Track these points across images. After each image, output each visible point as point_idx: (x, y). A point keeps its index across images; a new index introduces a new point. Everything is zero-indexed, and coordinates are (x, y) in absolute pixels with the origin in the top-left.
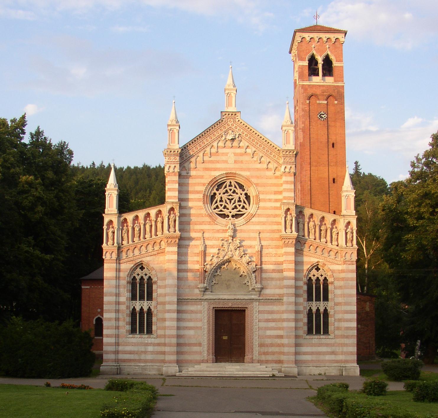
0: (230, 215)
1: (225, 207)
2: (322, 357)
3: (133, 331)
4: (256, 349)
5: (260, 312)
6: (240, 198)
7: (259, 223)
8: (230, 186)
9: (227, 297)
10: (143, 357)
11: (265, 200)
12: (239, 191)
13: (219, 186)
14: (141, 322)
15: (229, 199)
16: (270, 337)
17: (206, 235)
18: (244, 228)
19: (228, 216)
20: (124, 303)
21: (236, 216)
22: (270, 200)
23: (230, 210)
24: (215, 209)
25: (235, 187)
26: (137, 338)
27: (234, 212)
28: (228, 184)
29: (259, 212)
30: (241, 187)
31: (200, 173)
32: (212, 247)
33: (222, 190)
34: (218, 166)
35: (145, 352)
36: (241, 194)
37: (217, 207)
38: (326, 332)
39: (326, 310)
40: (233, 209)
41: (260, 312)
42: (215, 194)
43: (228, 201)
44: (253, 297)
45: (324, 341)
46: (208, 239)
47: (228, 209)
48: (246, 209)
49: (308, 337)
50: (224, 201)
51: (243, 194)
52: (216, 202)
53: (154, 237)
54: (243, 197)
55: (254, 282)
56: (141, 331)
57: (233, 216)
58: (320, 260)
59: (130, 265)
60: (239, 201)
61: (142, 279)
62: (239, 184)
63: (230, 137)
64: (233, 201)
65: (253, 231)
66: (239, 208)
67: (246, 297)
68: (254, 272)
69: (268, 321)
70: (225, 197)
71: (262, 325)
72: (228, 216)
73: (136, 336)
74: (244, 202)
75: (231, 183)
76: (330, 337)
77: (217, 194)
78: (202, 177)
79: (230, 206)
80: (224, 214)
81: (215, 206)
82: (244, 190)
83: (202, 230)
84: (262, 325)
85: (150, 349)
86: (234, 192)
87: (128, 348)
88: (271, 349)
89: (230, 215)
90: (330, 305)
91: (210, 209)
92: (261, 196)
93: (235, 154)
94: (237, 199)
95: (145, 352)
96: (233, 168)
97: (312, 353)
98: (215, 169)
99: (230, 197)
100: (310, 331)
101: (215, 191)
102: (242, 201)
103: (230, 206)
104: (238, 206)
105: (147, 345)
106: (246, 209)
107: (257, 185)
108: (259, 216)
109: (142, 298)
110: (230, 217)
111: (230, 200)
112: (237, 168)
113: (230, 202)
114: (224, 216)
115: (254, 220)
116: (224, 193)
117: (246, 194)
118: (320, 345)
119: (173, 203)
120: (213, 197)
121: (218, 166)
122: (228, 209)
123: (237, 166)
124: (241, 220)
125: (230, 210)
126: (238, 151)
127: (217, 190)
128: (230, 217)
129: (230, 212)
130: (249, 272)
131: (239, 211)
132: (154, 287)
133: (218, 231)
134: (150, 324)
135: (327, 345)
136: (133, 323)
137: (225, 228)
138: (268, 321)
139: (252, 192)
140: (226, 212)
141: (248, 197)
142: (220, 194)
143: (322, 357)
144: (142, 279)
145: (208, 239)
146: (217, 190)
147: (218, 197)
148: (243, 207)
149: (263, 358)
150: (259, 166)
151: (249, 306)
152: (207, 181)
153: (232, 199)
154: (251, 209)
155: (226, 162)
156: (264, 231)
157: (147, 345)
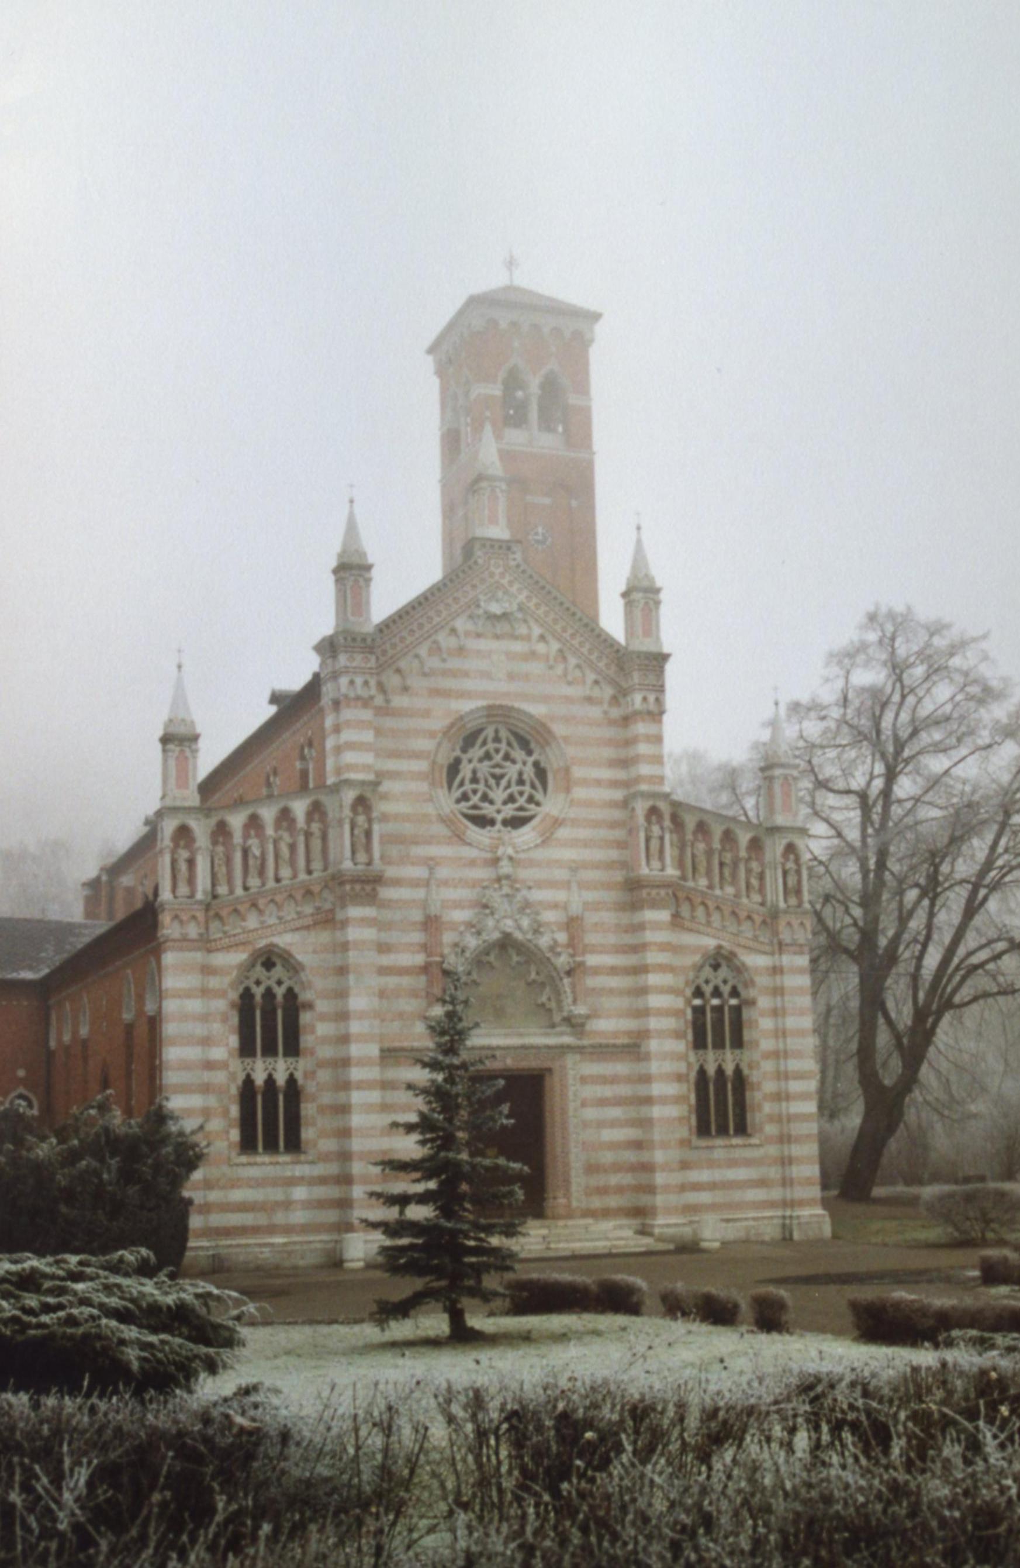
1: (485, 798)
2: (737, 1196)
3: (247, 1144)
4: (578, 1181)
5: (584, 1080)
6: (520, 774)
7: (574, 843)
8: (497, 739)
9: (499, 1039)
10: (280, 1218)
11: (585, 782)
12: (518, 754)
13: (470, 740)
14: (271, 1120)
15: (494, 776)
16: (614, 1146)
17: (443, 872)
18: (539, 854)
20: (223, 1065)
21: (516, 822)
22: (598, 783)
23: (498, 805)
25: (509, 744)
26: (264, 1166)
27: (509, 811)
28: (490, 732)
29: (572, 813)
30: (525, 744)
31: (420, 703)
32: (458, 905)
33: (477, 752)
34: (468, 684)
35: (287, 1205)
36: (524, 763)
37: (465, 797)
38: (742, 1129)
39: (738, 1071)
40: (505, 803)
41: (584, 1080)
42: (457, 761)
43: (492, 782)
44: (567, 1040)
45: (738, 1153)
46: (445, 883)
47: (491, 802)
48: (538, 804)
49: (703, 1143)
50: (482, 782)
52: (462, 784)
53: (302, 876)
54: (529, 772)
55: (570, 1000)
56: (271, 1146)
57: (506, 823)
58: (724, 943)
59: (240, 957)
60: (521, 782)
61: (269, 994)
62: (516, 735)
63: (495, 608)
64: (504, 782)
65: (559, 863)
67: (552, 1041)
68: (569, 973)
69: (602, 1102)
70: (484, 768)
71: (591, 1113)
72: (492, 822)
73: (259, 1159)
74: (533, 786)
75: (497, 731)
76: (754, 1141)
77: (464, 762)
78: (427, 713)
79: (499, 795)
81: (458, 794)
82: (530, 753)
83: (432, 859)
84: (591, 1113)
85: (300, 1193)
86: (507, 757)
87: (237, 1195)
88: (614, 1180)
89: (499, 818)
90: (746, 1056)
91: (446, 802)
92: (577, 772)
93: (510, 656)
94: (515, 777)
95: (287, 1205)
97: (713, 1186)
99: (497, 771)
100: (703, 1129)
101: (458, 753)
102: (528, 783)
103: (499, 795)
105: (292, 1182)
106: (538, 804)
107: (566, 739)
108: (575, 823)
109: (270, 1050)
111: (498, 778)
113: (498, 784)
114: (483, 822)
115: (563, 833)
117: (536, 764)
118: (732, 1163)
119: (363, 783)
120: (454, 768)
122: (491, 802)
126: (518, 647)
127: (464, 750)
129: (499, 812)
130: (554, 974)
132: (305, 1018)
133: (472, 863)
134: (294, 1122)
135: (748, 1163)
136: (247, 1123)
137: (489, 855)
138: (602, 1102)
139: (552, 760)
140: (488, 810)
141: (541, 773)
142: (470, 761)
143: (737, 1196)
144: (269, 994)
145: (445, 883)
146: (464, 750)
147: (466, 771)
148: (531, 799)
149: (596, 1203)
150: (570, 691)
151: (556, 1066)
152: (438, 723)
154: (552, 805)
155: (486, 675)
156: (585, 865)
157: (292, 1182)
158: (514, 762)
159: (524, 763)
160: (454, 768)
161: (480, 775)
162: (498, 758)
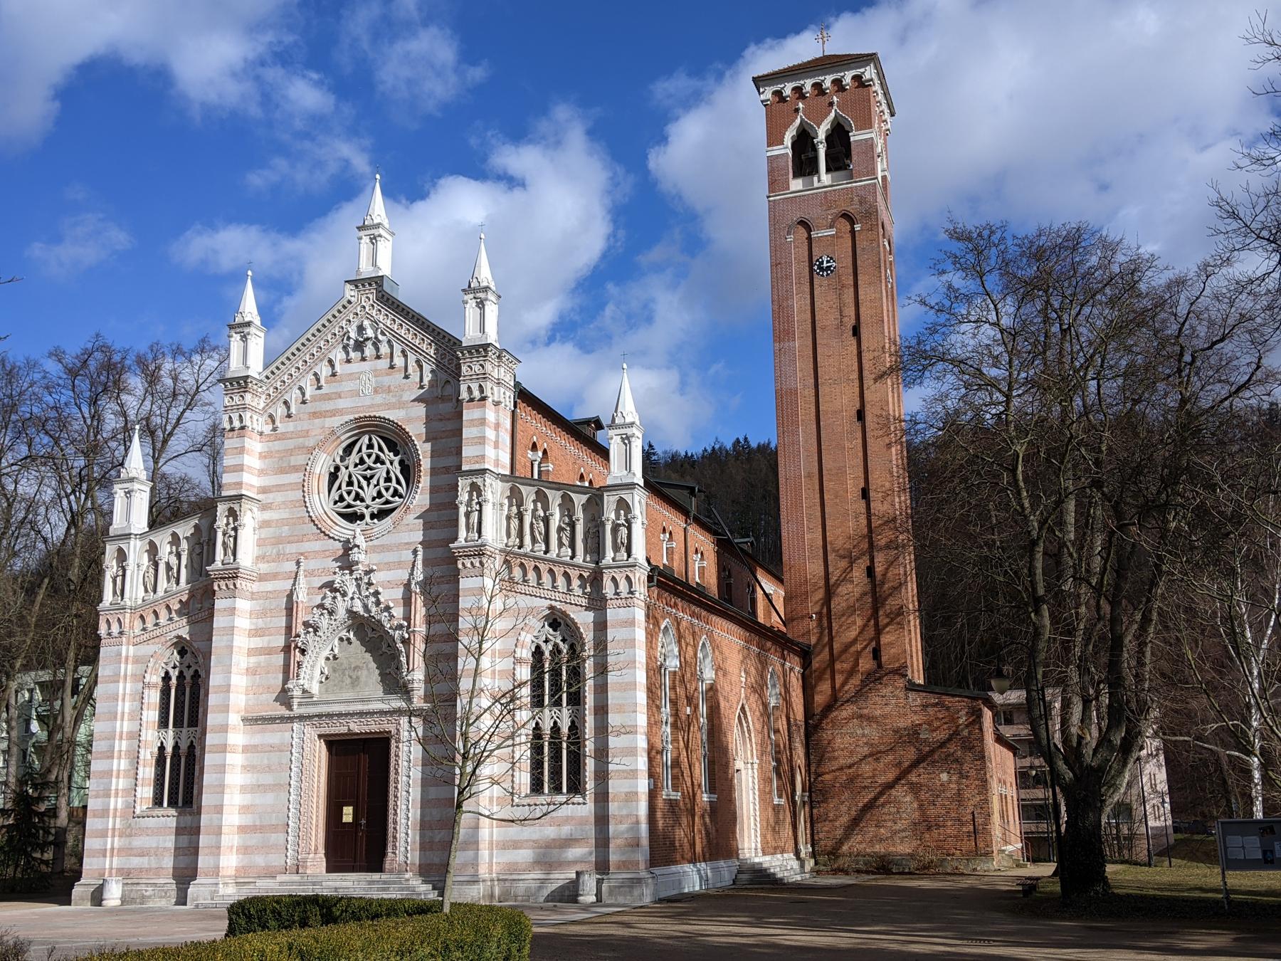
0: (367, 513)
1: (358, 497)
15: (365, 478)
19: (362, 517)
21: (381, 515)
24: (336, 503)
27: (376, 506)
31: (305, 425)
34: (342, 404)
37: (342, 499)
42: (337, 468)
51: (396, 464)
57: (373, 516)
64: (374, 481)
66: (387, 495)
72: (362, 517)
74: (398, 482)
75: (370, 439)
77: (343, 469)
79: (369, 492)
80: (355, 513)
89: (367, 513)
96: (370, 407)
98: (334, 413)
99: (369, 473)
103: (369, 492)
104: (384, 492)
110: (368, 518)
111: (368, 479)
112: (379, 405)
114: (353, 517)
116: (356, 465)
121: (342, 404)
122: (362, 500)
123: (379, 399)
124: (388, 521)
125: (369, 501)
128: (368, 518)
129: (367, 507)
131: (387, 502)
140: (359, 507)
146: (342, 459)
147: (343, 476)
148: (396, 493)
153: (372, 477)
155: (356, 394)
158: (383, 463)
159: (391, 463)
160: (333, 477)
161: (354, 479)
162: (370, 462)
